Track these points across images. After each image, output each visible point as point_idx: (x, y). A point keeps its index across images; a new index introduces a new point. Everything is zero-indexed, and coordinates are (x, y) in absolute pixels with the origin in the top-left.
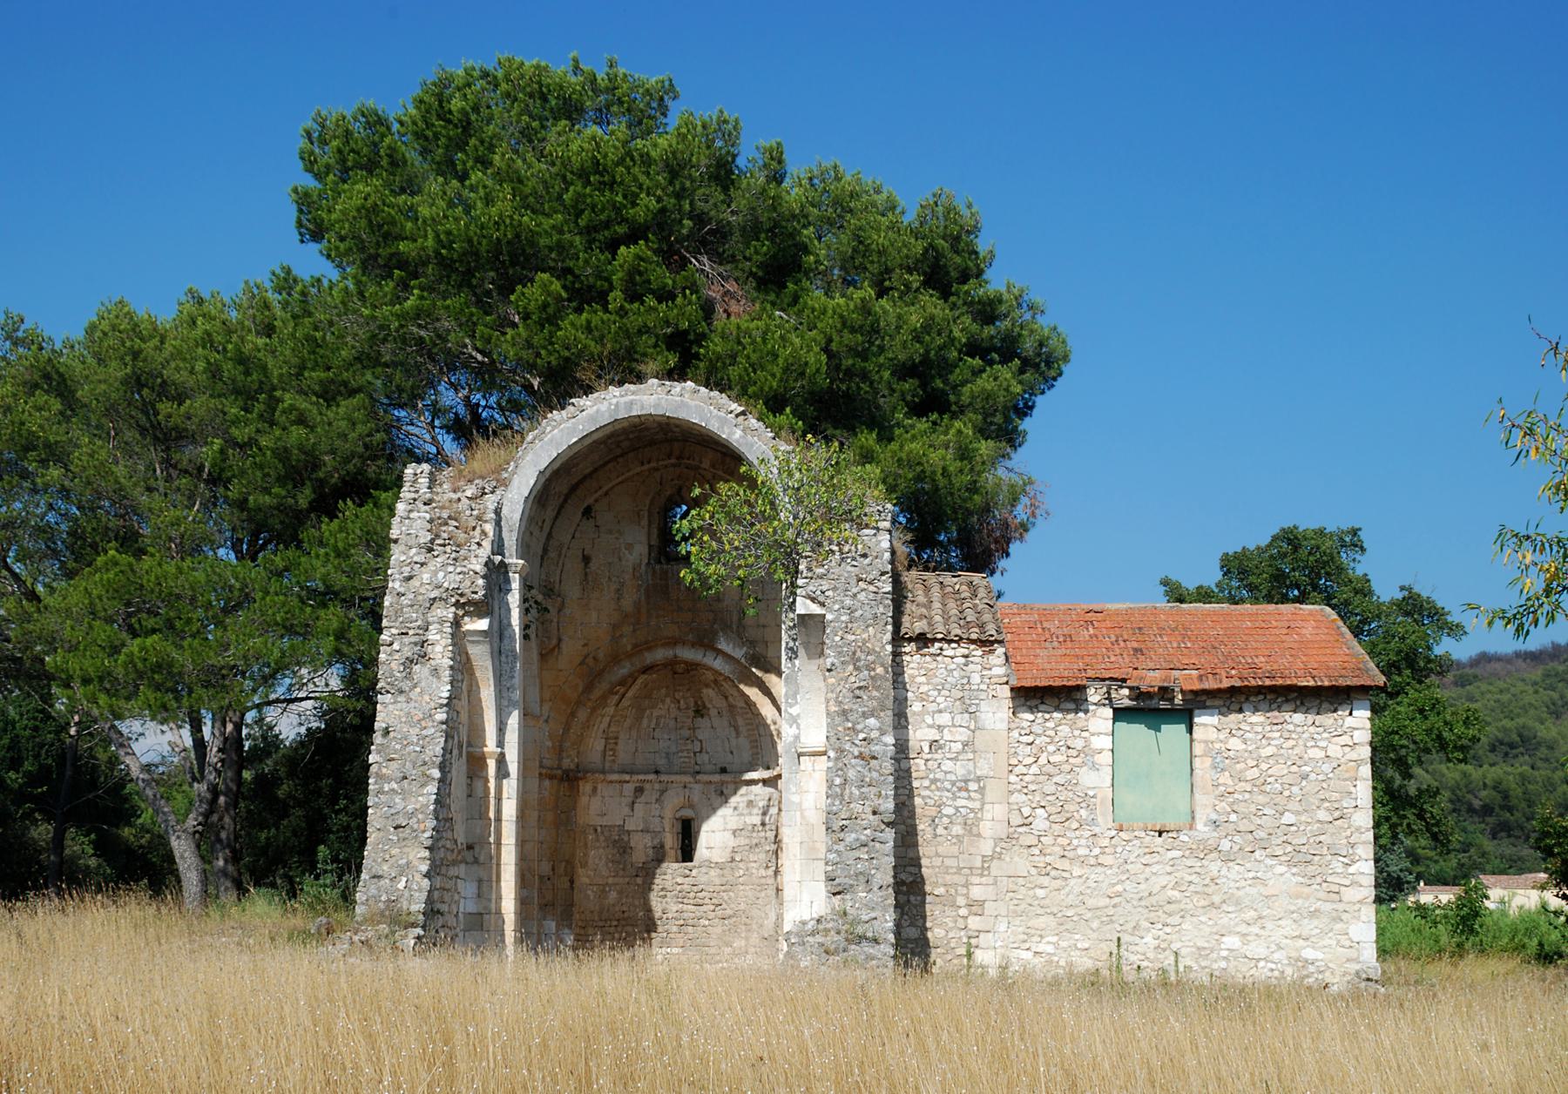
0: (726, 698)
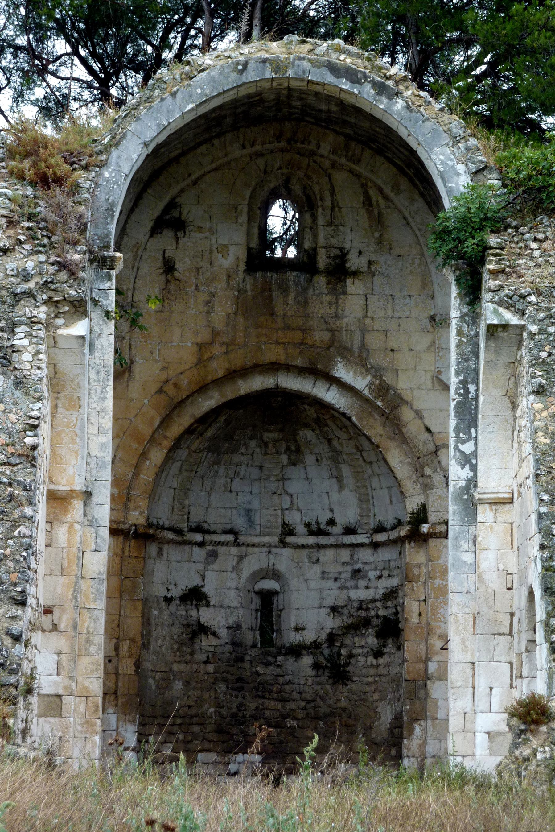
0: (329, 441)
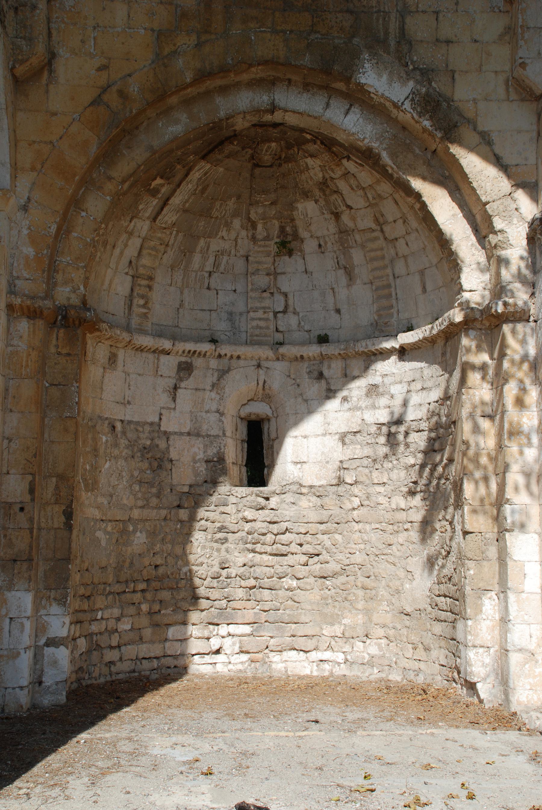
0: (337, 216)
